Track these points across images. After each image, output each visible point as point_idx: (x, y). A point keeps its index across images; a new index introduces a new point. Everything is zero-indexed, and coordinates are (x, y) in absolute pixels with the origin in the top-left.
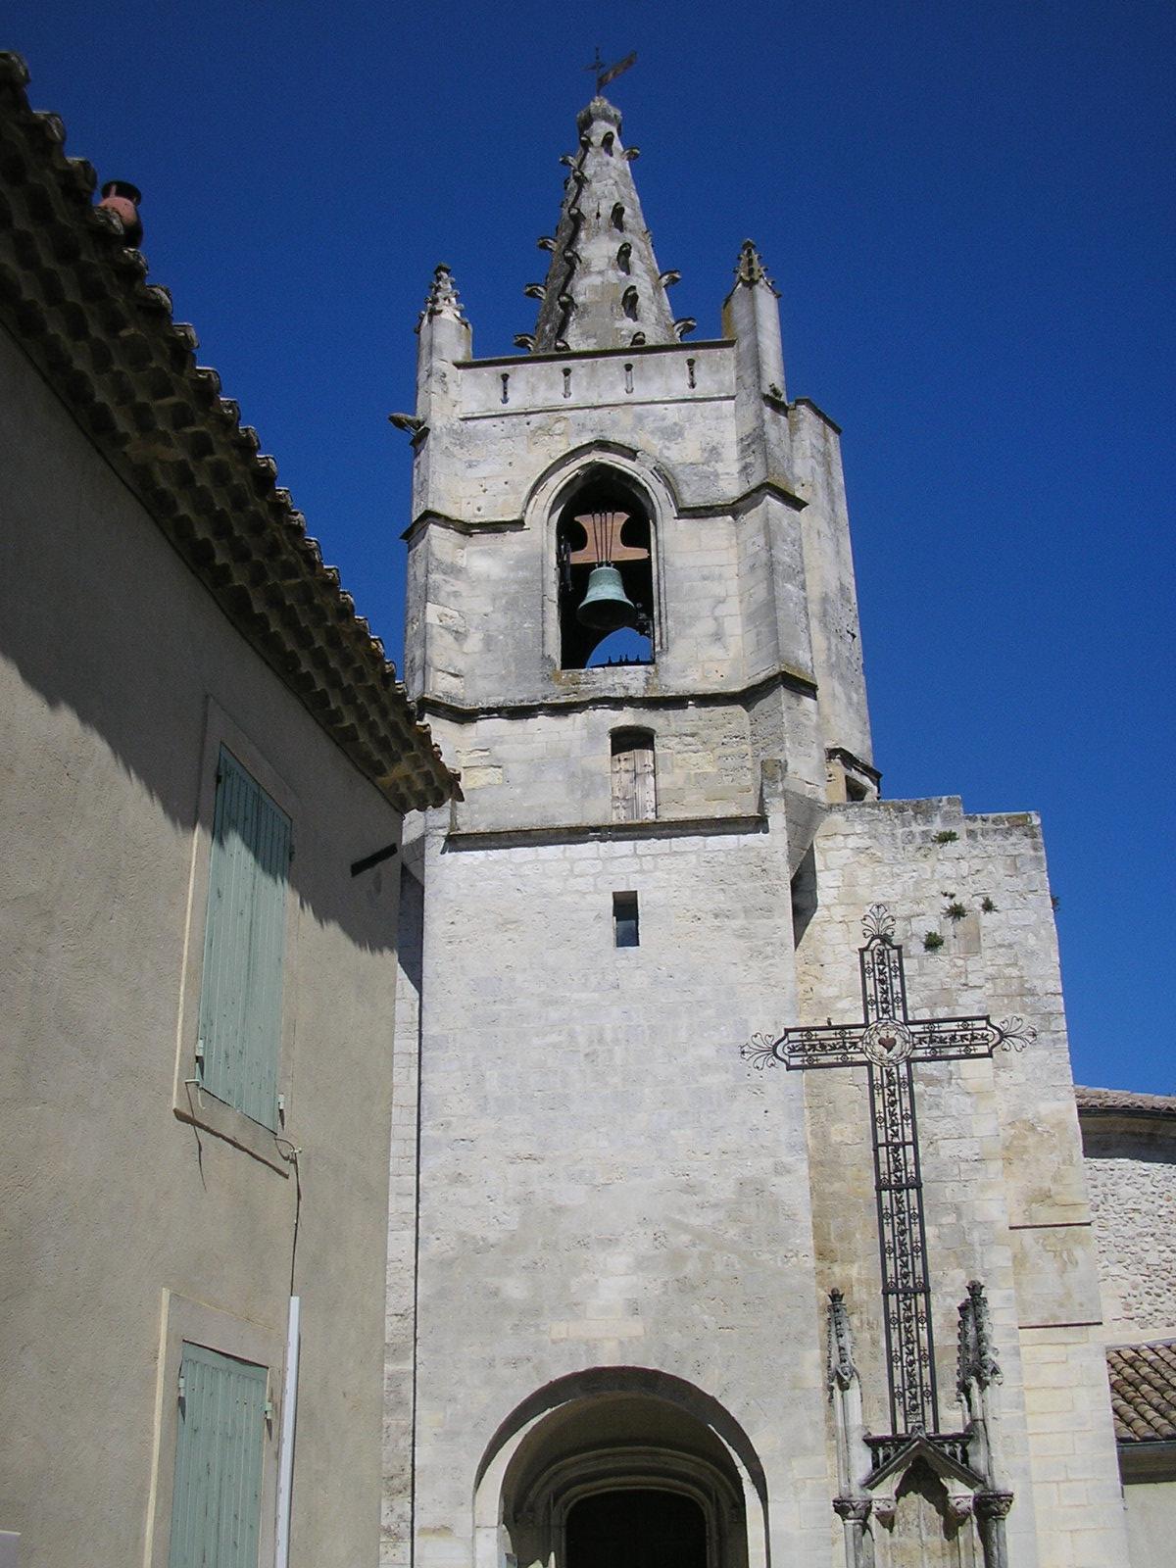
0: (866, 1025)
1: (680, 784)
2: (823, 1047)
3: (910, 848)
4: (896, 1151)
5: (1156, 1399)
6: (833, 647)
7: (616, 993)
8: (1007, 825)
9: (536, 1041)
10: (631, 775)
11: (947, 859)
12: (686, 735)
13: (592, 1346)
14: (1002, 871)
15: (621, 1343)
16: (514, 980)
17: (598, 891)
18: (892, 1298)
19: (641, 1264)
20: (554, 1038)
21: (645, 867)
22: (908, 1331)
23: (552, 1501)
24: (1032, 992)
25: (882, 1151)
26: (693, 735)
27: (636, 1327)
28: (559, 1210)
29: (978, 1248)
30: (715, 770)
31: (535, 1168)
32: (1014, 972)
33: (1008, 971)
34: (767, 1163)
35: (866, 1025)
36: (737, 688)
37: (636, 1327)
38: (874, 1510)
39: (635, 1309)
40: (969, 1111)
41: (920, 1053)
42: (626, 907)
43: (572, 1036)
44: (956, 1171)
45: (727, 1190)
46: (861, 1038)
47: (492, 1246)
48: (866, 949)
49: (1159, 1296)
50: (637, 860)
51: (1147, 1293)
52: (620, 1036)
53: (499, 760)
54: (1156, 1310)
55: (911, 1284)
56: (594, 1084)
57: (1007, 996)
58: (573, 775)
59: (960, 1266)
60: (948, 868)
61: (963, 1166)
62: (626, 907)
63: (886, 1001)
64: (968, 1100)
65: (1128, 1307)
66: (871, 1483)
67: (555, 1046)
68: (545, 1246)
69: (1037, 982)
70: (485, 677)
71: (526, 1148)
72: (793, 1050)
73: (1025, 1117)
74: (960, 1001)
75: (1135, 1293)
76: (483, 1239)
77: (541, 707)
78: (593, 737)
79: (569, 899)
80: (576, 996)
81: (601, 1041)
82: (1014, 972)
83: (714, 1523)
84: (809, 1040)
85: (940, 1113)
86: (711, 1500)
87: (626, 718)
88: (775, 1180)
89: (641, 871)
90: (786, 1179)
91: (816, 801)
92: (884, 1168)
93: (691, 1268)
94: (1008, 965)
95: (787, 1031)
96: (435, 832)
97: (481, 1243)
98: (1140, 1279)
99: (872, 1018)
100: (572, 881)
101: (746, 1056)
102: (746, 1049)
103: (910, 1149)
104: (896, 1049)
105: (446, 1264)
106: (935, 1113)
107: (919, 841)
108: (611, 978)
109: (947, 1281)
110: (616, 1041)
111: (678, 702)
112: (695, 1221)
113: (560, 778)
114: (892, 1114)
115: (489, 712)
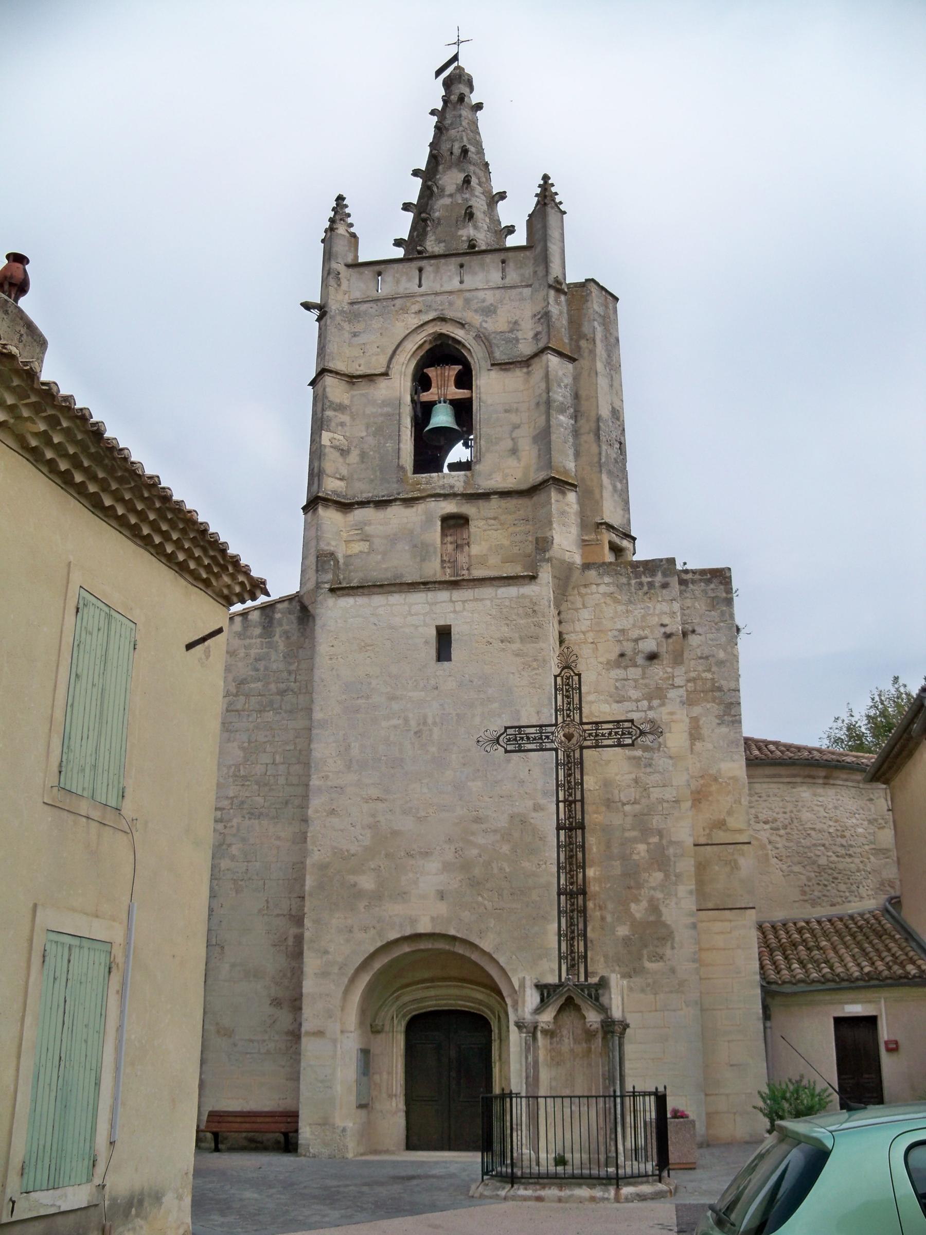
0: (556, 725)
1: (484, 552)
2: (528, 738)
3: (640, 593)
4: (570, 805)
5: (803, 954)
6: (604, 454)
7: (436, 692)
8: (709, 576)
9: (384, 724)
10: (454, 546)
11: (663, 600)
12: (490, 519)
13: (413, 921)
14: (704, 608)
16: (370, 684)
17: (426, 625)
18: (563, 898)
19: (447, 867)
20: (395, 722)
21: (457, 609)
22: (572, 918)
24: (720, 689)
25: (561, 805)
26: (495, 519)
27: (442, 909)
28: (395, 833)
29: (673, 859)
30: (508, 543)
31: (380, 806)
32: (709, 676)
33: (704, 675)
34: (530, 803)
35: (556, 725)
36: (524, 486)
37: (442, 909)
38: (539, 1028)
39: (442, 895)
40: (671, 769)
41: (588, 743)
42: (444, 636)
43: (406, 720)
44: (660, 808)
45: (502, 821)
46: (553, 733)
48: (558, 676)
49: (825, 886)
50: (451, 604)
51: (818, 884)
52: (437, 720)
53: (368, 536)
54: (824, 896)
55: (575, 889)
56: (419, 752)
57: (703, 692)
58: (415, 546)
59: (660, 870)
60: (665, 607)
61: (665, 805)
62: (444, 636)
63: (569, 709)
64: (671, 762)
65: (804, 893)
66: (538, 1011)
67: (395, 727)
68: (387, 855)
69: (723, 682)
70: (359, 480)
71: (374, 792)
72: (509, 740)
73: (711, 772)
74: (669, 696)
75: (810, 884)
76: (347, 851)
77: (395, 500)
78: (429, 520)
79: (407, 630)
80: (410, 694)
81: (425, 723)
82: (709, 676)
83: (497, 1031)
84: (520, 734)
85: (651, 770)
87: (450, 507)
88: (534, 814)
89: (455, 612)
90: (541, 814)
91: (573, 564)
92: (562, 816)
93: (477, 872)
94: (704, 671)
95: (506, 728)
96: (323, 586)
98: (813, 875)
99: (560, 719)
100: (409, 618)
101: (481, 743)
102: (480, 739)
103: (579, 805)
104: (574, 741)
105: (323, 867)
106: (648, 770)
107: (646, 588)
108: (433, 682)
109: (651, 880)
110: (435, 723)
111: (485, 496)
112: (481, 840)
113: (407, 548)
114: (569, 782)
115: (363, 504)
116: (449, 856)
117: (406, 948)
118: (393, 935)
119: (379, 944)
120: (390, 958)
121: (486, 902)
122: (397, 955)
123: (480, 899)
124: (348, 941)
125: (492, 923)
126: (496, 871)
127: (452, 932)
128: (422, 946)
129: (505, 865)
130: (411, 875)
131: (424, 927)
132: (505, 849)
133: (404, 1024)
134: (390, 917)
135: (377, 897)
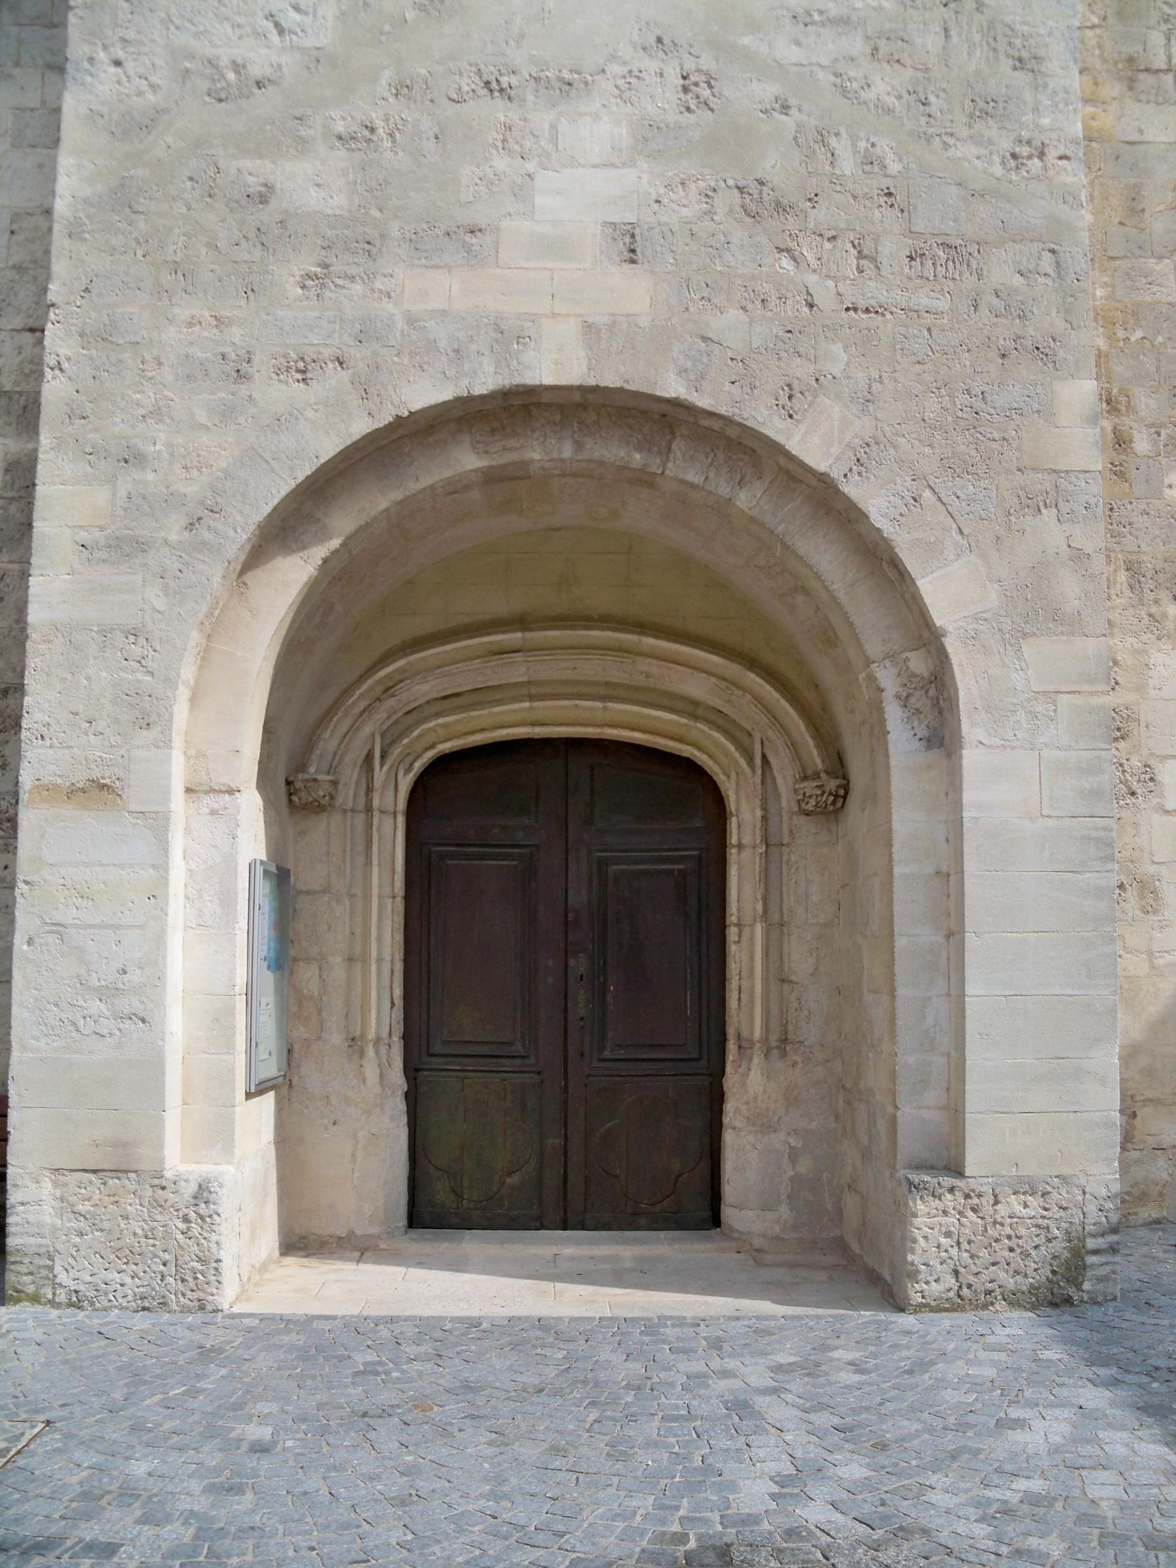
13: (509, 336)
15: (588, 327)
19: (650, 140)
23: (377, 754)
27: (633, 294)
37: (633, 294)
47: (259, 84)
68: (402, 89)
76: (236, 67)
86: (750, 761)
93: (776, 165)
97: (231, 76)
105: (133, 126)
116: (661, 100)
117: (467, 459)
118: (423, 393)
119: (360, 427)
120: (397, 495)
121: (811, 279)
122: (426, 481)
123: (786, 262)
124: (226, 413)
125: (837, 358)
126: (847, 165)
127: (673, 387)
128: (537, 451)
129: (884, 146)
130: (501, 163)
131: (555, 363)
132: (884, 85)
133: (406, 783)
134: (412, 320)
135: (354, 245)
